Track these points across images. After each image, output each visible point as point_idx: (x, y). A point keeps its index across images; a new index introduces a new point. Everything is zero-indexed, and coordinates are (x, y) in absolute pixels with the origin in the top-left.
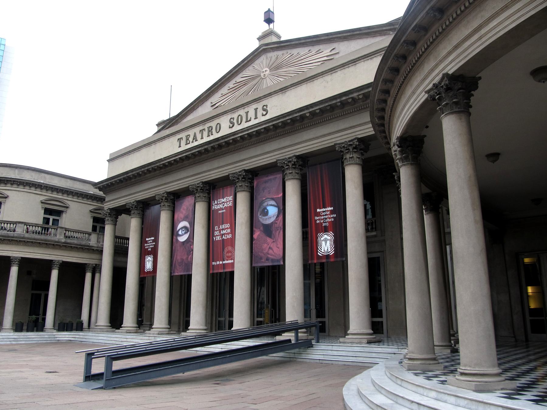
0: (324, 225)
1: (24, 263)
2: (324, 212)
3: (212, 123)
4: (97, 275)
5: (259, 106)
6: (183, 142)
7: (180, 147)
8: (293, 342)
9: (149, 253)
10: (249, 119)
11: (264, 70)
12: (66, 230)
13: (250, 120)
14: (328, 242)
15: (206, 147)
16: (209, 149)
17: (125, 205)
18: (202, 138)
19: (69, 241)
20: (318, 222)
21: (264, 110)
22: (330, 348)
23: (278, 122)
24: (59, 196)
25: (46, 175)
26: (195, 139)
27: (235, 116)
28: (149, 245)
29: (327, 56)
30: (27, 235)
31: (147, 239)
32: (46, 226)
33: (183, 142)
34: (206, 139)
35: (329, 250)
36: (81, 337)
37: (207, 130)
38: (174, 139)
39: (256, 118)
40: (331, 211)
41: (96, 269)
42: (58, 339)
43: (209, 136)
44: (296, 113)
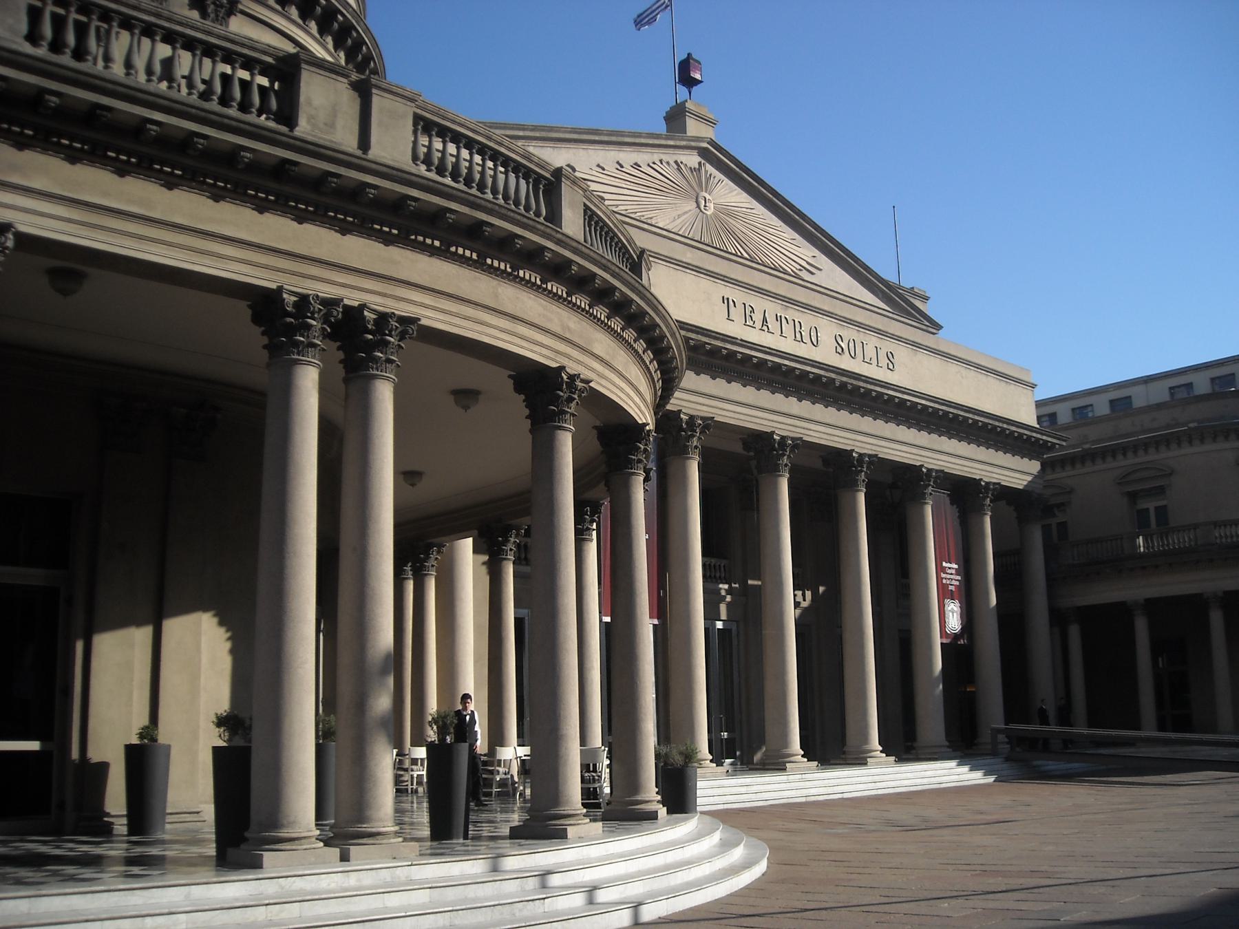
5: (888, 346)
6: (737, 313)
11: (708, 197)
34: (787, 345)
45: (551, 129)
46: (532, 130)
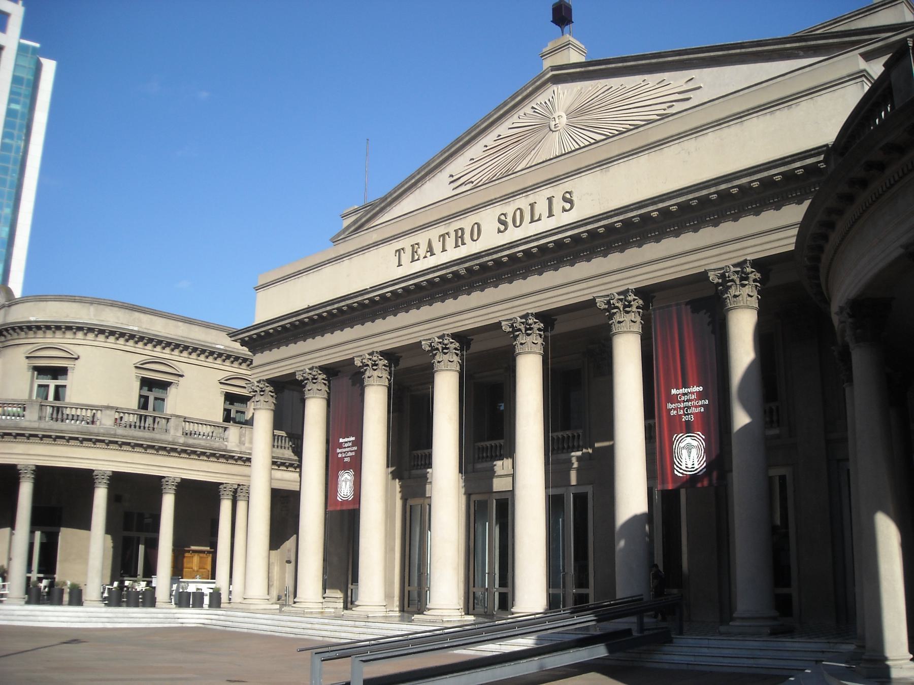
0: (684, 419)
1: (118, 481)
2: (684, 394)
3: (463, 221)
4: (241, 505)
5: (557, 192)
6: (406, 257)
7: (400, 265)
8: (635, 634)
9: (346, 467)
10: (536, 218)
11: (555, 115)
12: (185, 420)
13: (539, 219)
14: (694, 451)
15: (455, 269)
16: (463, 272)
17: (294, 374)
18: (444, 250)
19: (191, 441)
20: (673, 413)
21: (565, 199)
22: (705, 642)
23: (596, 225)
24: (166, 354)
25: (142, 316)
26: (431, 250)
27: (509, 209)
28: (345, 451)
29: (679, 93)
30: (120, 431)
31: (341, 440)
32: (143, 412)
33: (406, 257)
34: (454, 254)
35: (696, 466)
36: (222, 618)
37: (453, 235)
38: (389, 250)
39: (551, 215)
40: (698, 393)
41: (238, 494)
42: (180, 621)
43: (457, 246)
44: (632, 210)
45: (428, 164)
46: (419, 173)
